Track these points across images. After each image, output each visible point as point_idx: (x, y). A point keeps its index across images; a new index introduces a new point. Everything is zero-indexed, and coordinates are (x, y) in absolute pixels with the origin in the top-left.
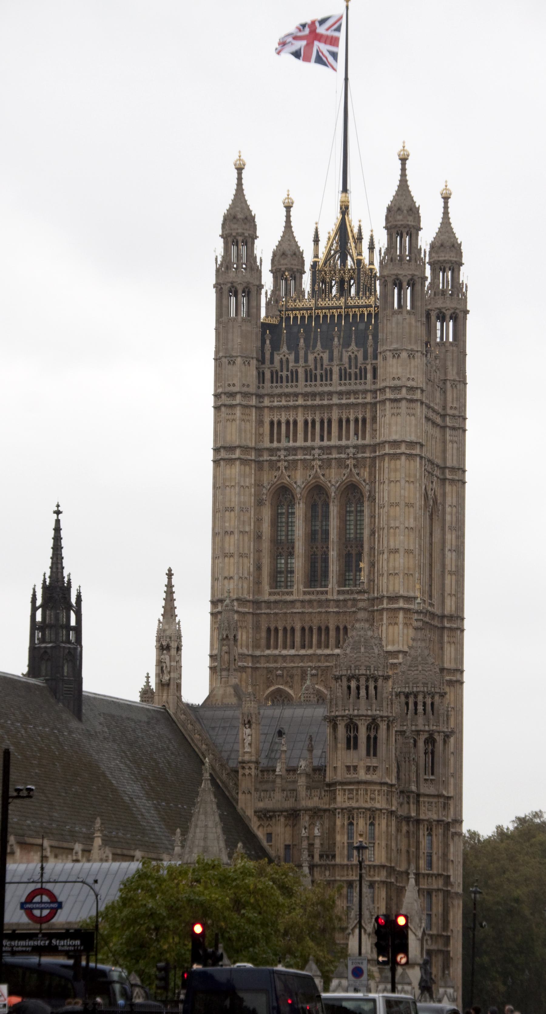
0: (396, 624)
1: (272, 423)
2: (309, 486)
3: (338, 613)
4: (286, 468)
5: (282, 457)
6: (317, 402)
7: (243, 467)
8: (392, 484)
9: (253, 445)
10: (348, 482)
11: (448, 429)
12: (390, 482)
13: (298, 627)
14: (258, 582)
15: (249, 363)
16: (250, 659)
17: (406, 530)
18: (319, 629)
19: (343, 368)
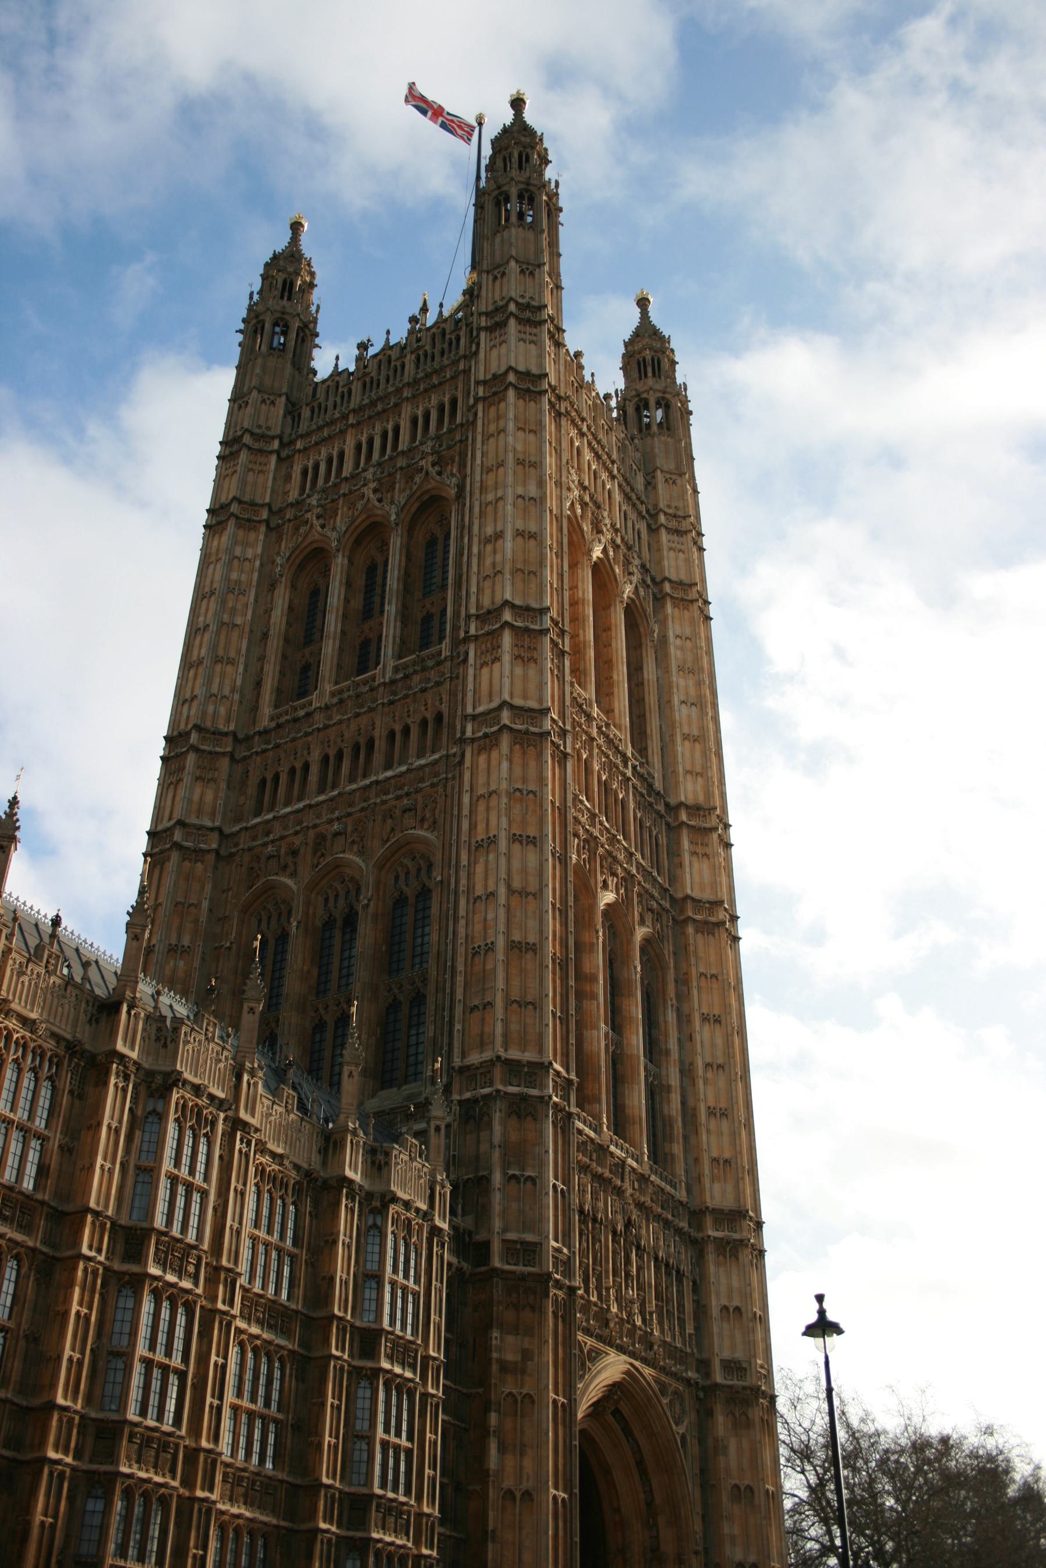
0: (497, 659)
1: (305, 472)
2: (357, 527)
3: (391, 703)
4: (318, 517)
5: (314, 502)
6: (379, 407)
7: (241, 533)
8: (492, 440)
9: (267, 500)
10: (422, 495)
11: (663, 531)
12: (487, 437)
13: (315, 756)
14: (255, 708)
15: (273, 403)
16: (215, 836)
17: (520, 500)
18: (356, 748)
19: (421, 353)
